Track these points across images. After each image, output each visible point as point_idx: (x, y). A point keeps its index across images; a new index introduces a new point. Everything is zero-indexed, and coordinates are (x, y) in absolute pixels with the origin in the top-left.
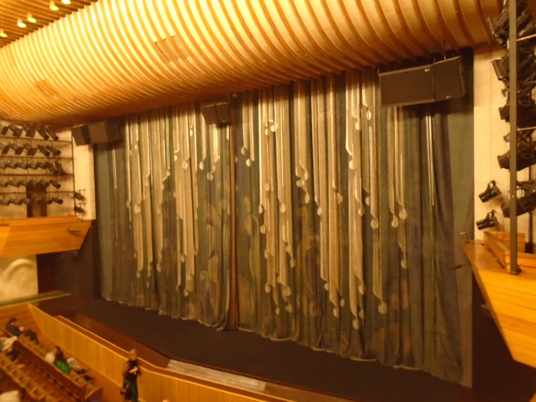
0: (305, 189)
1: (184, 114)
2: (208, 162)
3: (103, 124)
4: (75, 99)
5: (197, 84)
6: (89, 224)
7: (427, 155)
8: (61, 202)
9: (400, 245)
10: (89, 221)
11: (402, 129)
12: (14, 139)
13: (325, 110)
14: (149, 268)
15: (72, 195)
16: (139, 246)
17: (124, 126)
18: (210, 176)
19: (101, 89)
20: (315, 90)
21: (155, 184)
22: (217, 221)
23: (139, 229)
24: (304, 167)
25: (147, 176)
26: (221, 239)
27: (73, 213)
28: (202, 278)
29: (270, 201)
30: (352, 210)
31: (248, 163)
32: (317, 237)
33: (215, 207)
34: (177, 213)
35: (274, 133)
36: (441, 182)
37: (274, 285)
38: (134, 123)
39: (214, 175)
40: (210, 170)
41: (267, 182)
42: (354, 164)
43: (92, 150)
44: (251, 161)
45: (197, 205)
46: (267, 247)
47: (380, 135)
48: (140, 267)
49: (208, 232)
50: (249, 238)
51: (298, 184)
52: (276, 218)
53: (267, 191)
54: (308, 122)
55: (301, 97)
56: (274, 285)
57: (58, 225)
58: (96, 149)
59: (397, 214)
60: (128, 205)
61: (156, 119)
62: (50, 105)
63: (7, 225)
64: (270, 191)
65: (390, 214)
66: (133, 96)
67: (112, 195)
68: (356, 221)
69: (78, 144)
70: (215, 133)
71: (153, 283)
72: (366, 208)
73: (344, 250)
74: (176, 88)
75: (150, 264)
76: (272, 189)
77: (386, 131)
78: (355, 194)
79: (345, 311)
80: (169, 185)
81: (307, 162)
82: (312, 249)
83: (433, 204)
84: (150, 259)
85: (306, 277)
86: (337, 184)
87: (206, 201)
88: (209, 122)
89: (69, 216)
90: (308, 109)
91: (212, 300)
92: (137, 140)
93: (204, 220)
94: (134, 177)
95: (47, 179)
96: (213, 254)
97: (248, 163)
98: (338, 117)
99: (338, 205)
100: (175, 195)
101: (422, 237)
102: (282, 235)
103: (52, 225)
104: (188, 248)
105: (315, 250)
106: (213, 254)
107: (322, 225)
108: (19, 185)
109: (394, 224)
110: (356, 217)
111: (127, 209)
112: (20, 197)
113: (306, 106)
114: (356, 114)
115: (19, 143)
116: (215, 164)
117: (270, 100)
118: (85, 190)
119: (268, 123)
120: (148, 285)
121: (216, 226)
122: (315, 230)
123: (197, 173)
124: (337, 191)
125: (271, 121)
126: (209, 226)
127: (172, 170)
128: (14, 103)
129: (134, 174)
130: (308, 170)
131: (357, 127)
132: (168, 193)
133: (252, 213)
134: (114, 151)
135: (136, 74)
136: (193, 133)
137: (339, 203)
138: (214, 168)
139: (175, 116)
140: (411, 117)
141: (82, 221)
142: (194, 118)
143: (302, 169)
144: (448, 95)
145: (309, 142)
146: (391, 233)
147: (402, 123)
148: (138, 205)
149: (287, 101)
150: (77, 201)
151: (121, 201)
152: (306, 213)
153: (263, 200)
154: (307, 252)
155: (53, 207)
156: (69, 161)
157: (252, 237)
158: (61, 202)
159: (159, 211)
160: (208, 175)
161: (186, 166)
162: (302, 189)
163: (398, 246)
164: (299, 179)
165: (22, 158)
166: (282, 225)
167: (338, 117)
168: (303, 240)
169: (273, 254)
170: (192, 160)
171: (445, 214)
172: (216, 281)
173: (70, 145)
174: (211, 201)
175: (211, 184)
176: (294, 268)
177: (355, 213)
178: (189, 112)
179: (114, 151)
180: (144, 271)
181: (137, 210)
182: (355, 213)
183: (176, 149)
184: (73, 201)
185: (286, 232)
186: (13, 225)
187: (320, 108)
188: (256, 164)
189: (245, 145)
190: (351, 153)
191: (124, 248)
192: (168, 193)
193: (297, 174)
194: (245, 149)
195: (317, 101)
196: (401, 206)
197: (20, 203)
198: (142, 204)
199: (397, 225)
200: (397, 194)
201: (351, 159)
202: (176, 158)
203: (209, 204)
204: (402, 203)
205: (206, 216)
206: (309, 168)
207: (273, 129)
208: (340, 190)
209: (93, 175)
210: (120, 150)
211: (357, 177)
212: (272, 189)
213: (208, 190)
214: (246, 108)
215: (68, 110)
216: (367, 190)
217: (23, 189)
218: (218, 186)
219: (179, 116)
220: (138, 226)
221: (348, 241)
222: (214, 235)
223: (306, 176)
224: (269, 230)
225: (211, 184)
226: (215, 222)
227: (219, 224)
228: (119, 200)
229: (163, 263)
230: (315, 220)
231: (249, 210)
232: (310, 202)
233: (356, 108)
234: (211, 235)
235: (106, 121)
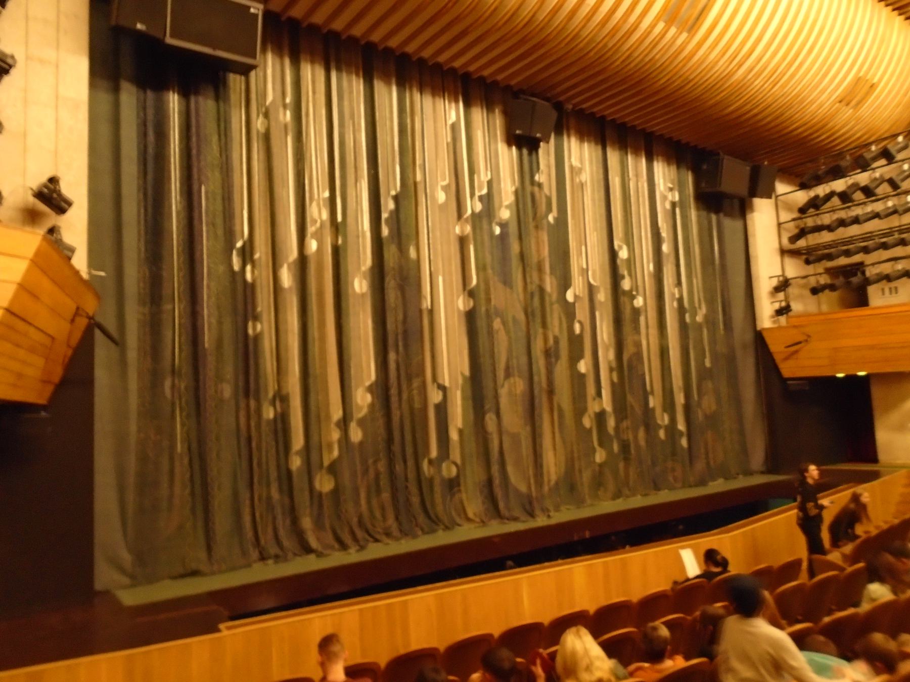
2: (488, 200)
21: (350, 220)
34: (424, 292)
56: (592, 415)
59: (700, 308)
72: (680, 300)
73: (664, 352)
79: (671, 428)
87: (490, 271)
91: (510, 469)
96: (508, 375)
105: (638, 355)
106: (508, 375)
107: (642, 319)
111: (236, 278)
125: (580, 166)
131: (668, 206)
134: (176, 96)
146: (699, 327)
149: (599, 148)
159: (359, 285)
160: (494, 224)
161: (441, 197)
185: (605, 332)
190: (664, 234)
193: (616, 247)
202: (419, 177)
212: (585, 266)
218: (515, 248)
230: (636, 312)
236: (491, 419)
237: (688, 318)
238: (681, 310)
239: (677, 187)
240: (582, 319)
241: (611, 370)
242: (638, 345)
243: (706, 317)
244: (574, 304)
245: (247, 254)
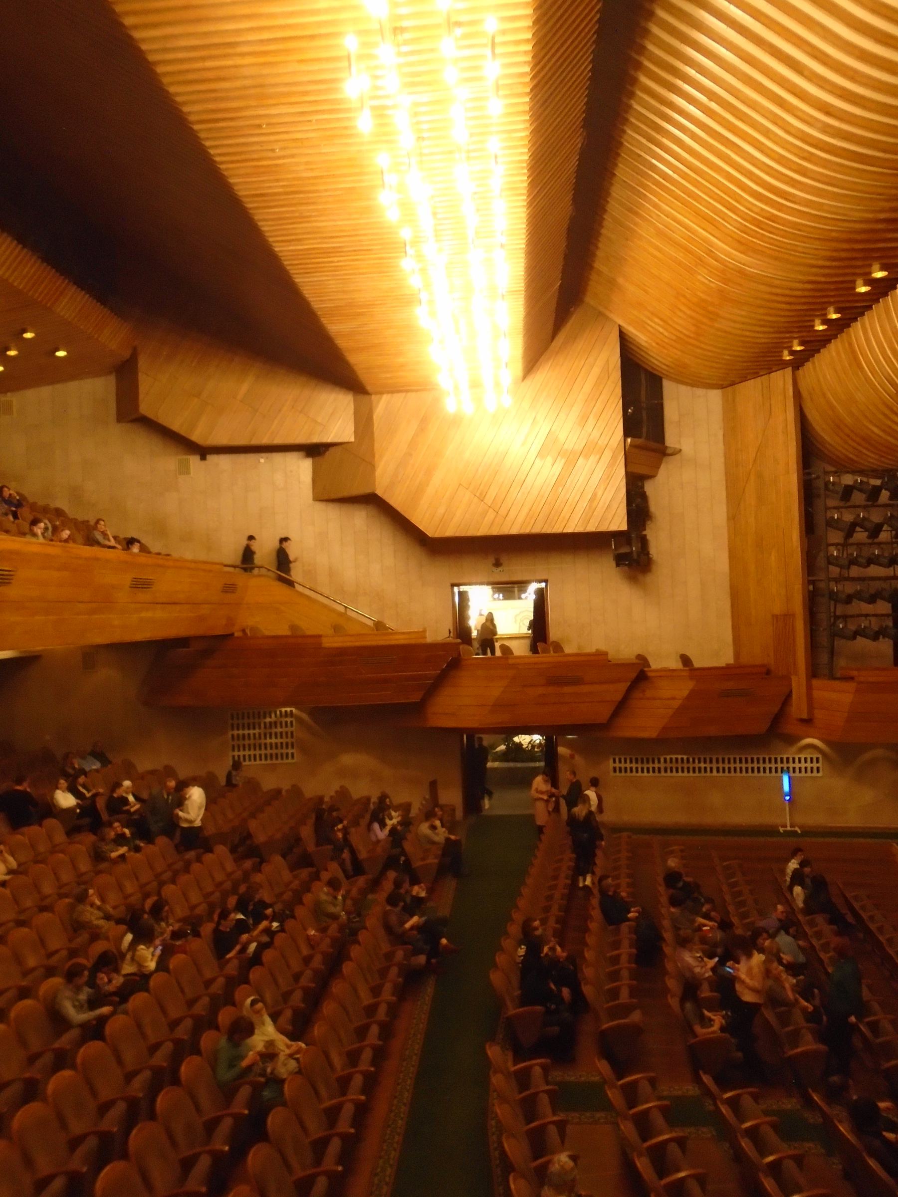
12: (865, 507)
63: (852, 678)
108: (872, 599)
112: (875, 624)
115: (876, 517)
128: (864, 439)
165: (879, 544)
186: (862, 679)
197: (875, 637)
217: (883, 607)
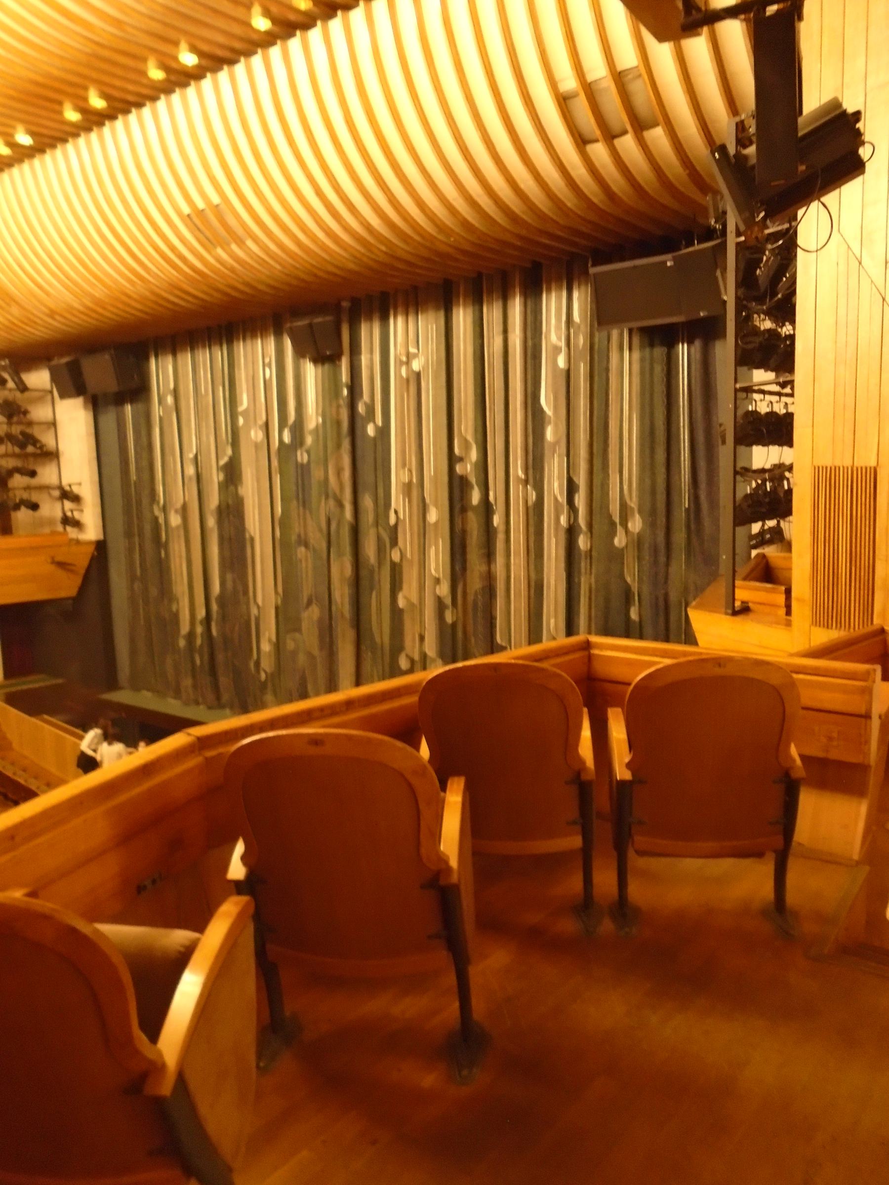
0: (473, 480)
1: (254, 336)
2: (298, 429)
3: (107, 357)
4: (52, 314)
5: (269, 286)
6: (91, 549)
7: (679, 416)
8: (35, 507)
9: (629, 580)
10: (89, 543)
11: (636, 367)
13: (505, 331)
14: (199, 629)
15: (56, 493)
16: (180, 588)
17: (147, 359)
18: (302, 455)
19: (97, 295)
20: (490, 293)
21: (204, 472)
22: (317, 540)
23: (180, 557)
24: (470, 438)
25: (191, 456)
26: (326, 573)
27: (60, 528)
28: (290, 645)
29: (410, 502)
30: (549, 517)
31: (371, 430)
32: (492, 566)
33: (311, 513)
35: (418, 375)
36: (702, 464)
37: (416, 657)
38: (165, 353)
39: (308, 452)
40: (302, 443)
41: (404, 465)
42: (556, 432)
43: (90, 407)
44: (376, 426)
45: (279, 510)
46: (405, 586)
47: (596, 378)
48: (185, 629)
49: (301, 561)
50: (372, 572)
51: (459, 469)
52: (422, 531)
53: (404, 484)
54: (478, 353)
55: (465, 306)
56: (416, 657)
57: (35, 549)
58: (96, 404)
60: (157, 512)
61: (204, 347)
62: (6, 323)
64: (410, 482)
65: (613, 524)
66: (155, 306)
67: (126, 495)
68: (556, 536)
69: (63, 396)
70: (311, 372)
71: (206, 657)
74: (234, 293)
75: (201, 622)
76: (414, 480)
77: (607, 370)
78: (555, 486)
80: (232, 473)
81: (476, 430)
82: (483, 588)
83: (687, 506)
84: (201, 613)
85: (473, 640)
86: (526, 470)
87: (295, 502)
88: (299, 353)
89: (54, 533)
90: (478, 329)
92: (172, 386)
93: (294, 538)
94: (169, 459)
95: (11, 463)
97: (371, 430)
98: (530, 343)
99: (527, 508)
100: (242, 491)
101: (667, 564)
102: (430, 565)
103: (23, 551)
104: (264, 590)
105: (490, 590)
109: (619, 541)
110: (556, 529)
113: (474, 322)
114: (559, 339)
116: (311, 432)
117: (411, 310)
118: (80, 484)
119: (408, 355)
120: (198, 662)
121: (314, 550)
122: (489, 555)
123: (279, 449)
124: (526, 482)
125: (413, 350)
126: (303, 549)
127: (235, 443)
129: (167, 451)
130: (476, 443)
131: (561, 362)
132: (232, 488)
133: (377, 524)
135: (157, 268)
136: (271, 373)
137: (530, 503)
138: (309, 440)
139: (238, 340)
140: (652, 345)
141: (78, 542)
142: (271, 343)
143: (466, 441)
144: (702, 309)
145: (479, 391)
147: (636, 355)
148: (176, 511)
150: (68, 505)
151: (145, 501)
152: (473, 523)
153: (397, 500)
154: (476, 594)
155: (22, 516)
156: (49, 428)
157: (376, 569)
158: (35, 507)
159: (211, 522)
160: (299, 453)
162: (467, 479)
163: (626, 582)
164: (461, 459)
166: (430, 547)
167: (530, 343)
168: (468, 572)
169: (415, 599)
170: (270, 424)
171: (707, 522)
172: (316, 652)
173: (49, 397)
174: (305, 503)
175: (304, 471)
176: (454, 625)
177: (554, 523)
178: (264, 335)
179: (128, 408)
180: (191, 636)
181: (175, 520)
182: (554, 523)
183: (242, 404)
184: (58, 505)
187: (498, 328)
188: (384, 432)
189: (366, 397)
190: (548, 410)
191: (154, 591)
192: (232, 488)
193: (457, 451)
194: (365, 403)
195: (492, 313)
196: (632, 509)
198: (184, 510)
199: (624, 544)
200: (625, 487)
201: (550, 423)
202: (241, 421)
203: (301, 508)
204: (633, 503)
205: (297, 530)
206: (480, 437)
207: (416, 365)
208: (531, 480)
209: (94, 454)
210: (140, 406)
211: (559, 456)
212: (414, 480)
213: (300, 482)
214: (368, 324)
215: (39, 333)
216: (575, 479)
218: (317, 474)
219: (244, 340)
220: (177, 549)
221: (542, 574)
222: (310, 565)
223: (474, 455)
224: (409, 555)
225: (304, 471)
226: (312, 542)
227: (324, 545)
228: (139, 503)
229: (224, 618)
231: (371, 517)
232: (480, 502)
233: (558, 327)
234: (307, 567)
235: (112, 352)
236: (294, 640)
237: (583, 542)
238: (572, 532)
239: (583, 327)
240: (402, 548)
241: (440, 606)
242: (490, 578)
243: (638, 542)
244: (396, 525)
245: (158, 503)
